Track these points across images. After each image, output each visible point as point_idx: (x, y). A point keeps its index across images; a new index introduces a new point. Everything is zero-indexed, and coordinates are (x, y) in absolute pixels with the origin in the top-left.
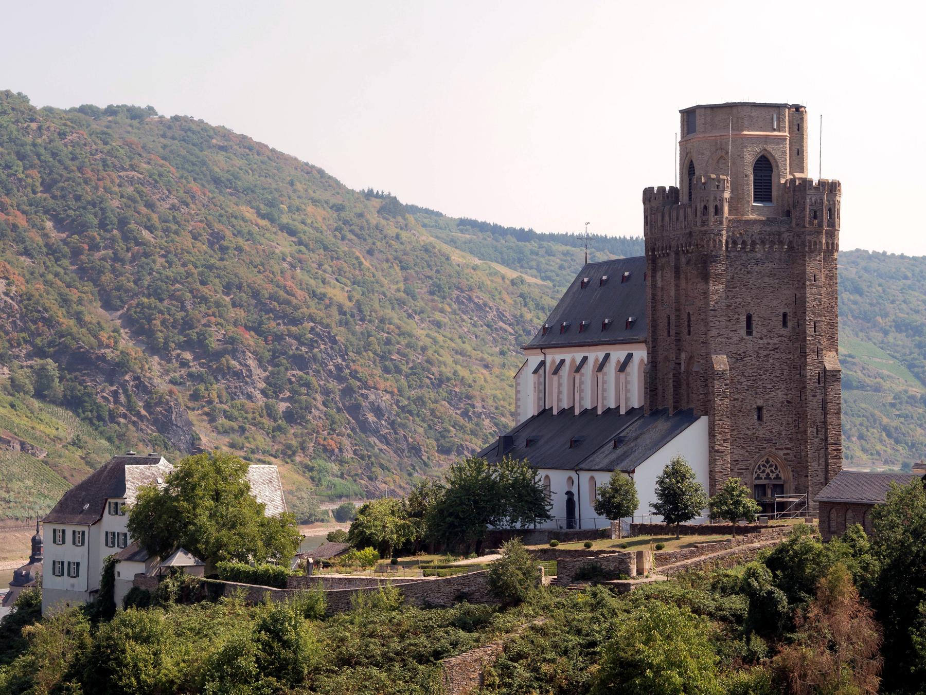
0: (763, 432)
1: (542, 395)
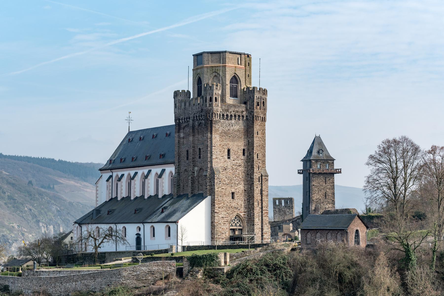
1: (111, 191)
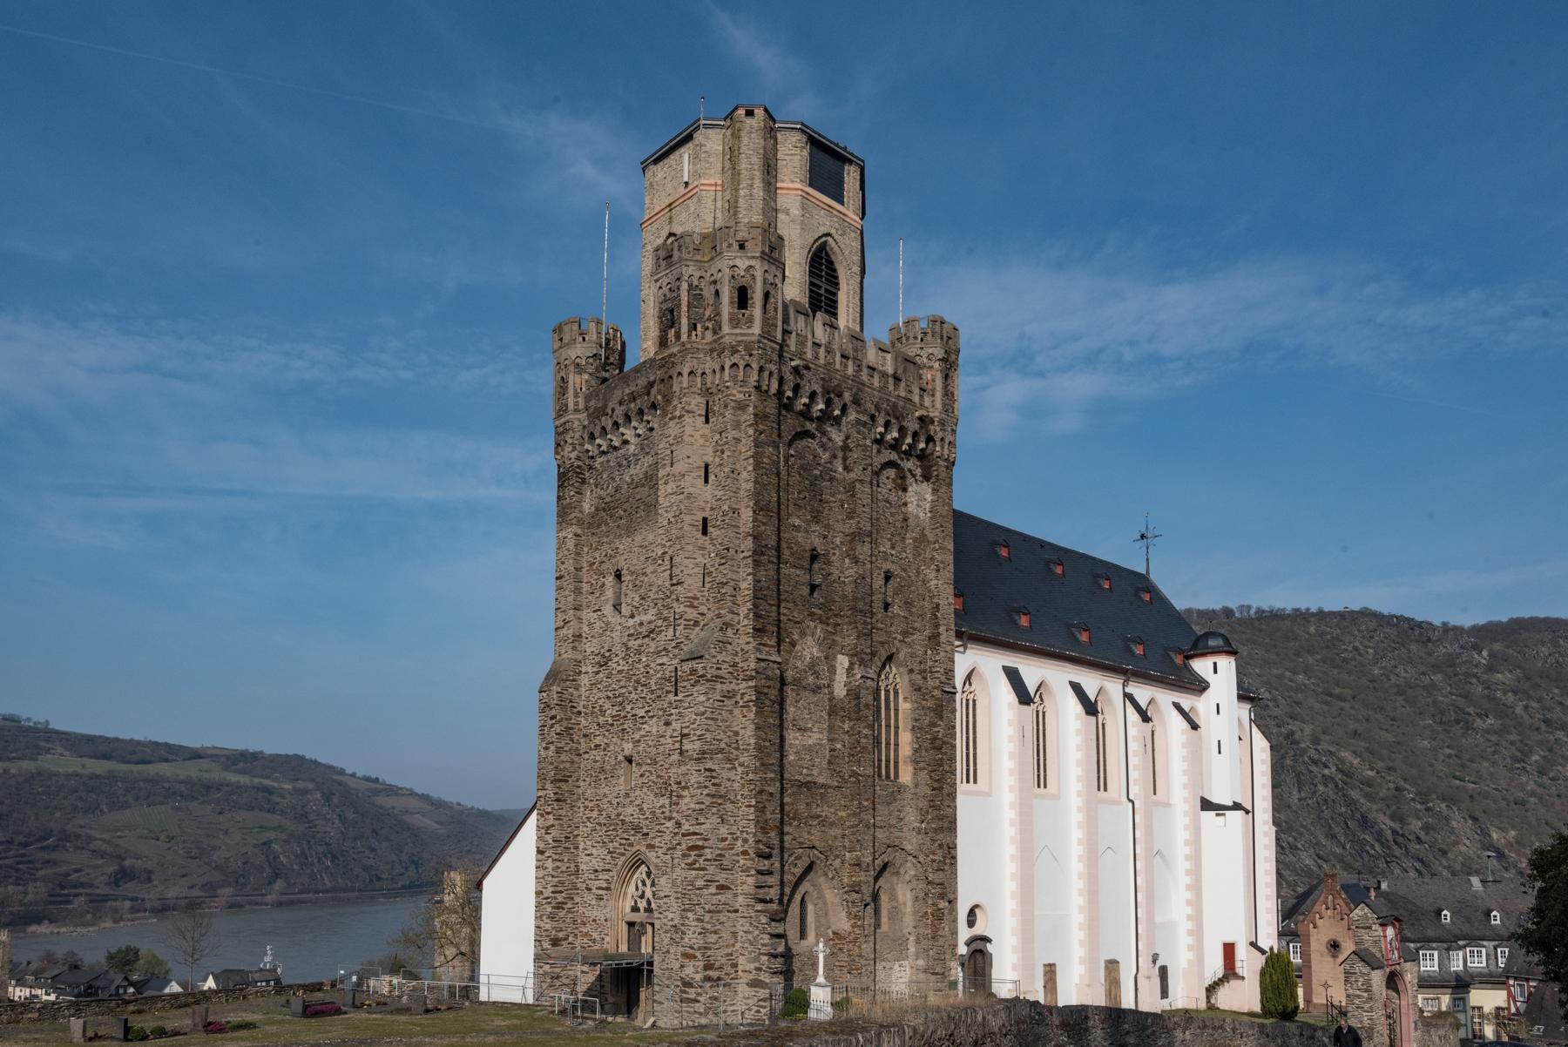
0: (630, 810)
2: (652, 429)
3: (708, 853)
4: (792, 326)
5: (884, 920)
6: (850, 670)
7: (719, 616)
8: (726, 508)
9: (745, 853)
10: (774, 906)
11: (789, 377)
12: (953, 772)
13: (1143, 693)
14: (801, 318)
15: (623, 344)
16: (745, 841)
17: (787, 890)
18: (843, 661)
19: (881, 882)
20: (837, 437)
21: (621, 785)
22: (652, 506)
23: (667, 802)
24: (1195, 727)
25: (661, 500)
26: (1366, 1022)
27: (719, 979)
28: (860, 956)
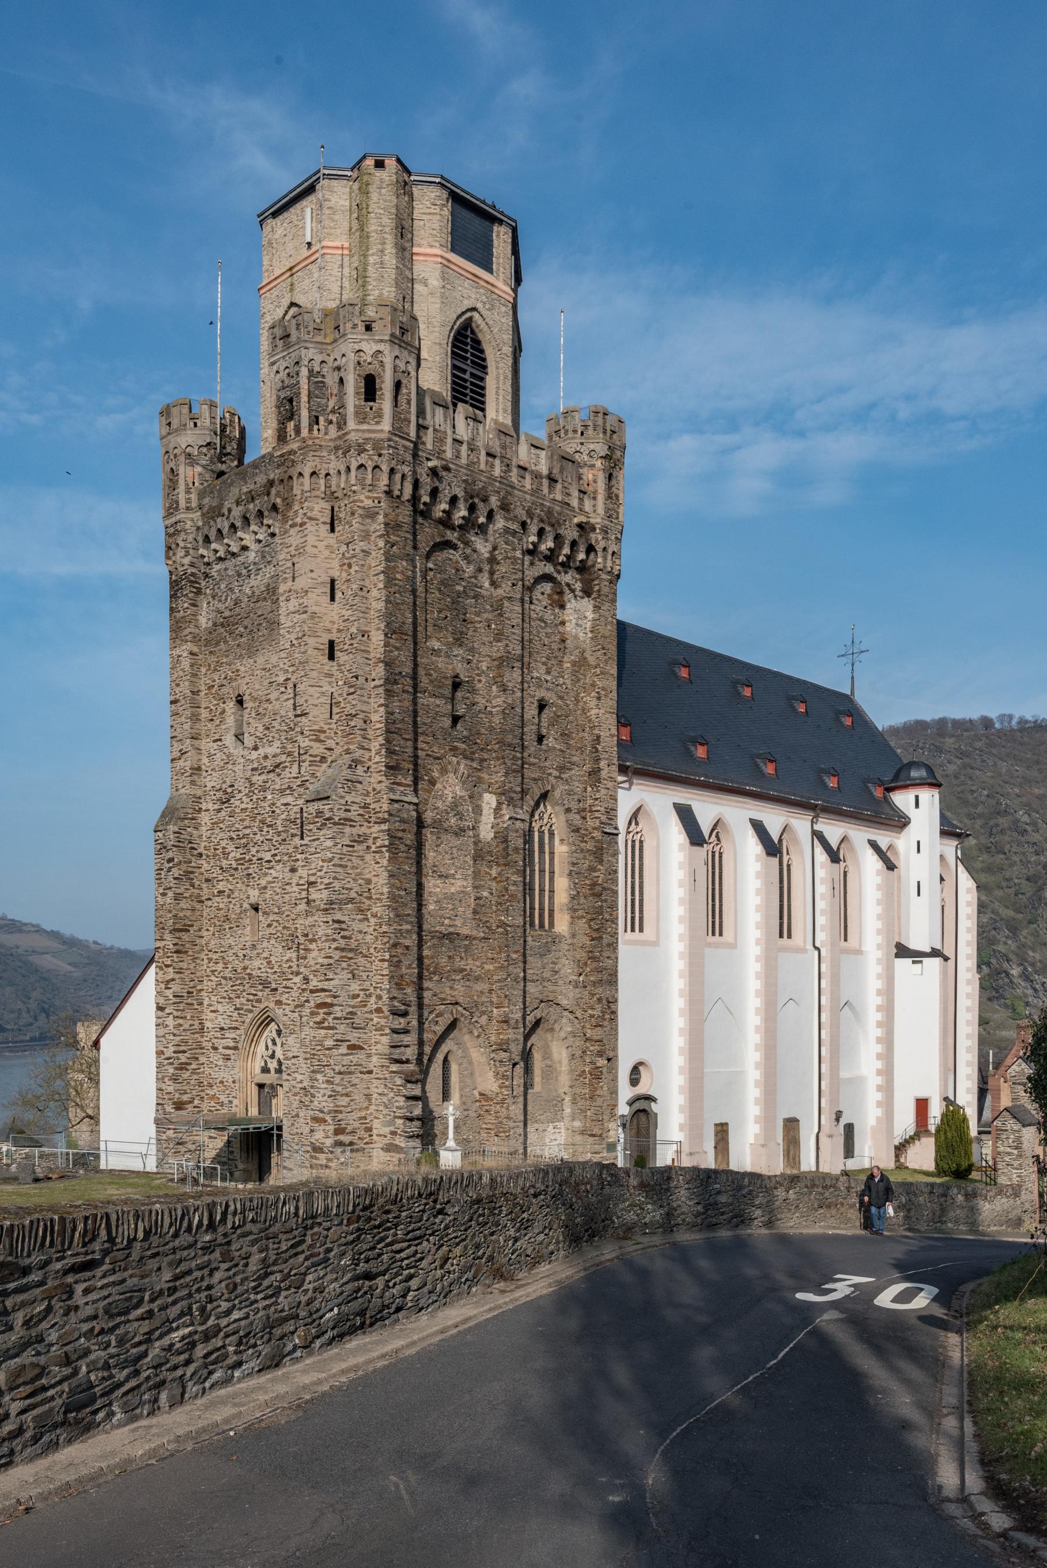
0: (257, 963)
2: (273, 535)
3: (338, 1011)
4: (429, 421)
5: (537, 1079)
6: (497, 810)
7: (348, 752)
8: (354, 630)
9: (379, 1010)
10: (412, 1067)
11: (425, 479)
12: (614, 921)
13: (833, 830)
14: (439, 411)
15: (243, 430)
16: (379, 997)
17: (427, 1049)
18: (489, 801)
19: (533, 1039)
20: (483, 548)
21: (247, 935)
22: (274, 624)
23: (294, 955)
24: (891, 866)
25: (283, 619)
26: (1015, 1180)
27: (351, 1144)
28: (508, 1118)
